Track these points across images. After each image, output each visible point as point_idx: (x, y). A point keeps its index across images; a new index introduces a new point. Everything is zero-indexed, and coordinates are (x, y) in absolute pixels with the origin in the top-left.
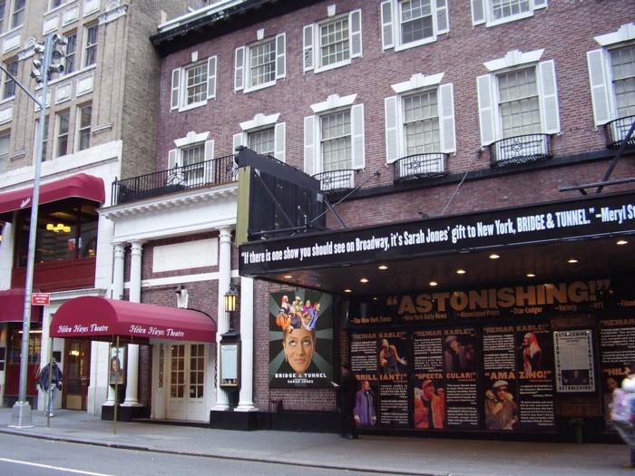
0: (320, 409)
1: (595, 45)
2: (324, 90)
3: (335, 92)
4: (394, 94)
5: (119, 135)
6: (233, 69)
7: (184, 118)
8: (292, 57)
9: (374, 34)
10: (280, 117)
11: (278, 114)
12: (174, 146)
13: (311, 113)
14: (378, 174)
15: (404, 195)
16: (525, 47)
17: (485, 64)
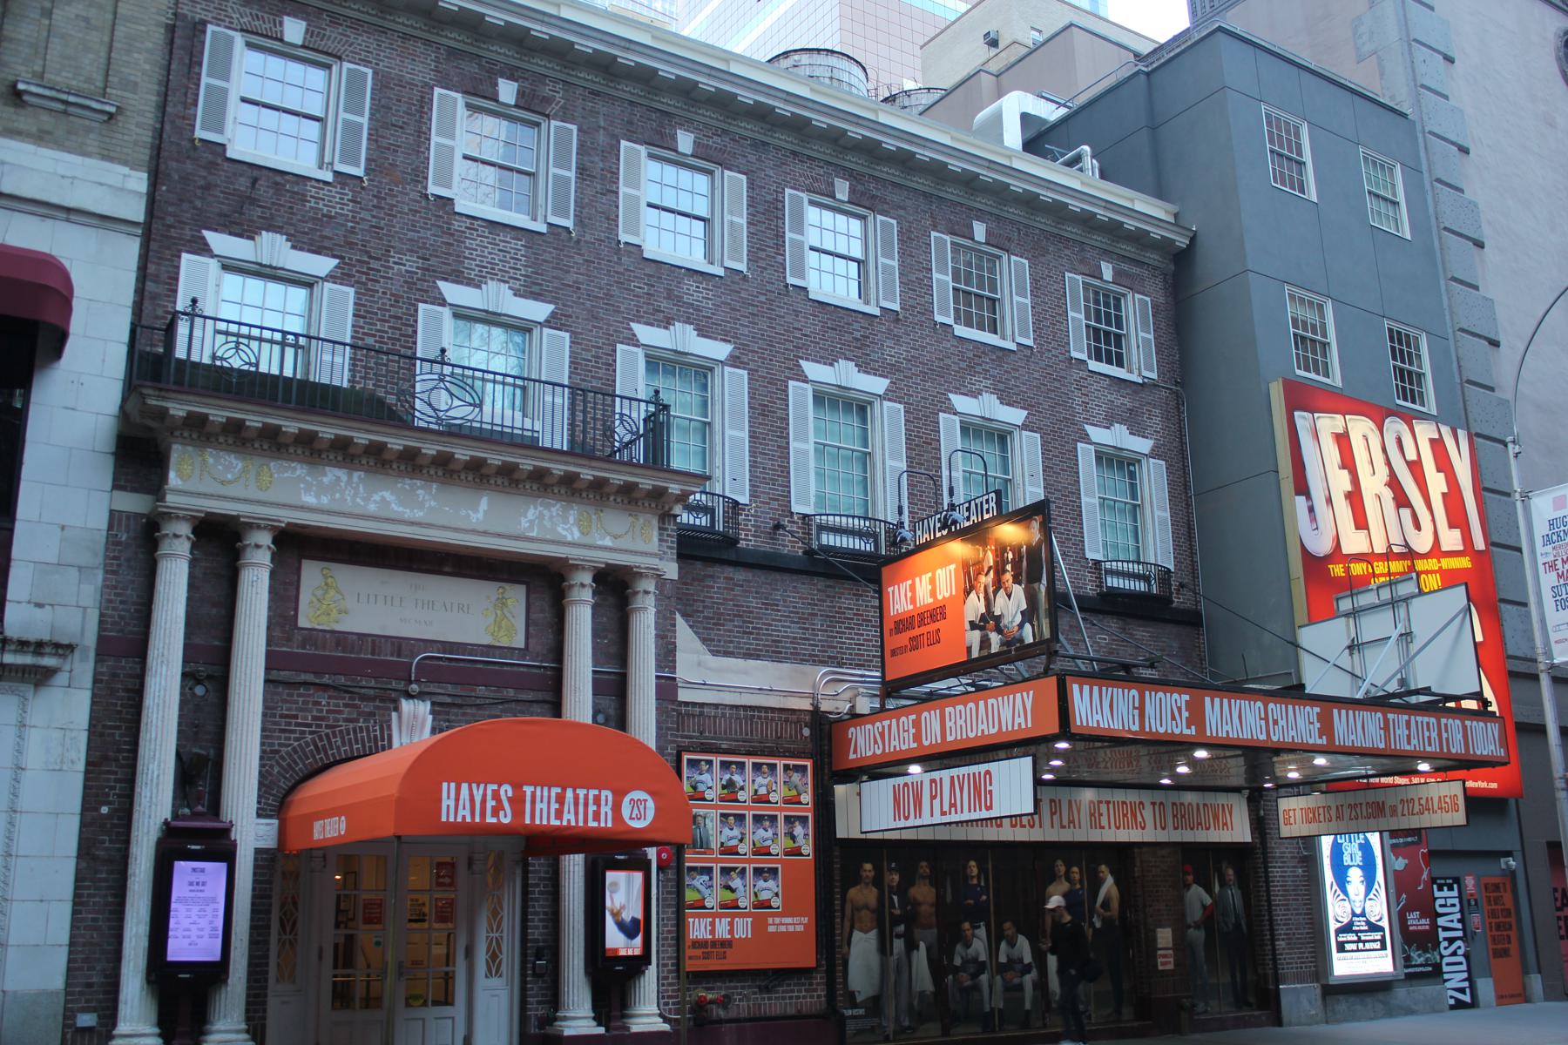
0: (791, 1011)
1: (1086, 438)
2: (664, 304)
3: (688, 321)
4: (806, 381)
5: (144, 154)
6: (423, 135)
7: (243, 183)
8: (589, 192)
9: (770, 243)
10: (553, 315)
11: (551, 307)
12: (203, 249)
13: (633, 341)
14: (778, 527)
15: (820, 583)
16: (1006, 400)
17: (951, 396)
